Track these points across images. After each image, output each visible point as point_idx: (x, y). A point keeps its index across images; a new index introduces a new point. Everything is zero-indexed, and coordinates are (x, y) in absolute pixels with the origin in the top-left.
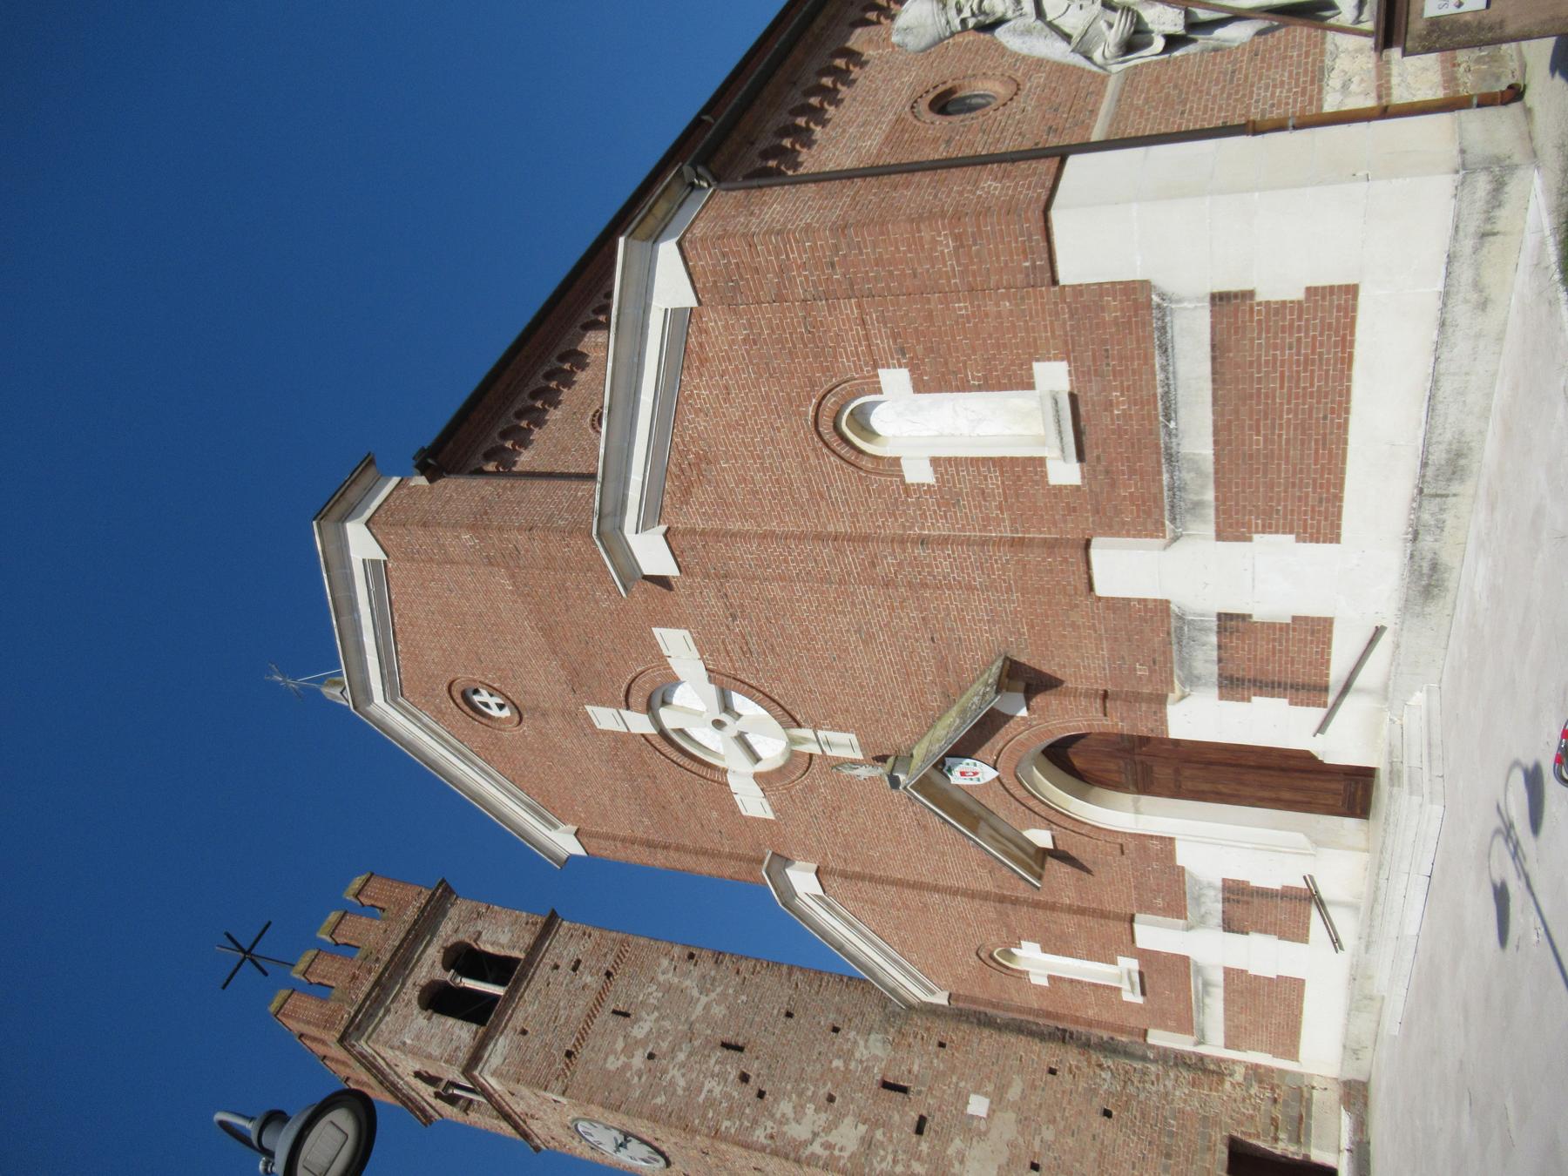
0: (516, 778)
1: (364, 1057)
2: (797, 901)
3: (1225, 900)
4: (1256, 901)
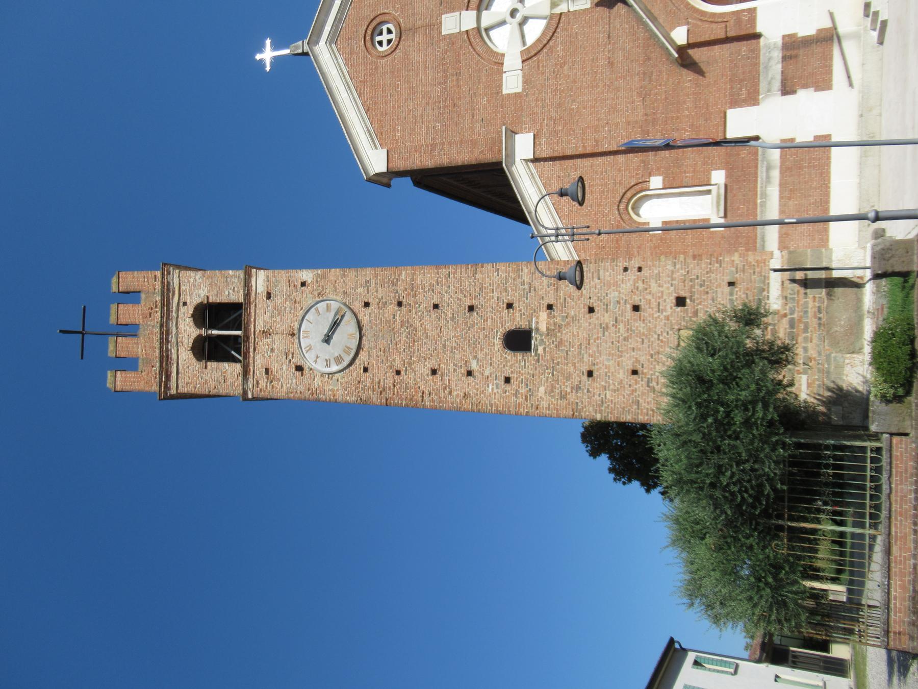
0: (370, 110)
1: (168, 290)
2: (514, 169)
3: (784, 58)
4: (801, 52)
